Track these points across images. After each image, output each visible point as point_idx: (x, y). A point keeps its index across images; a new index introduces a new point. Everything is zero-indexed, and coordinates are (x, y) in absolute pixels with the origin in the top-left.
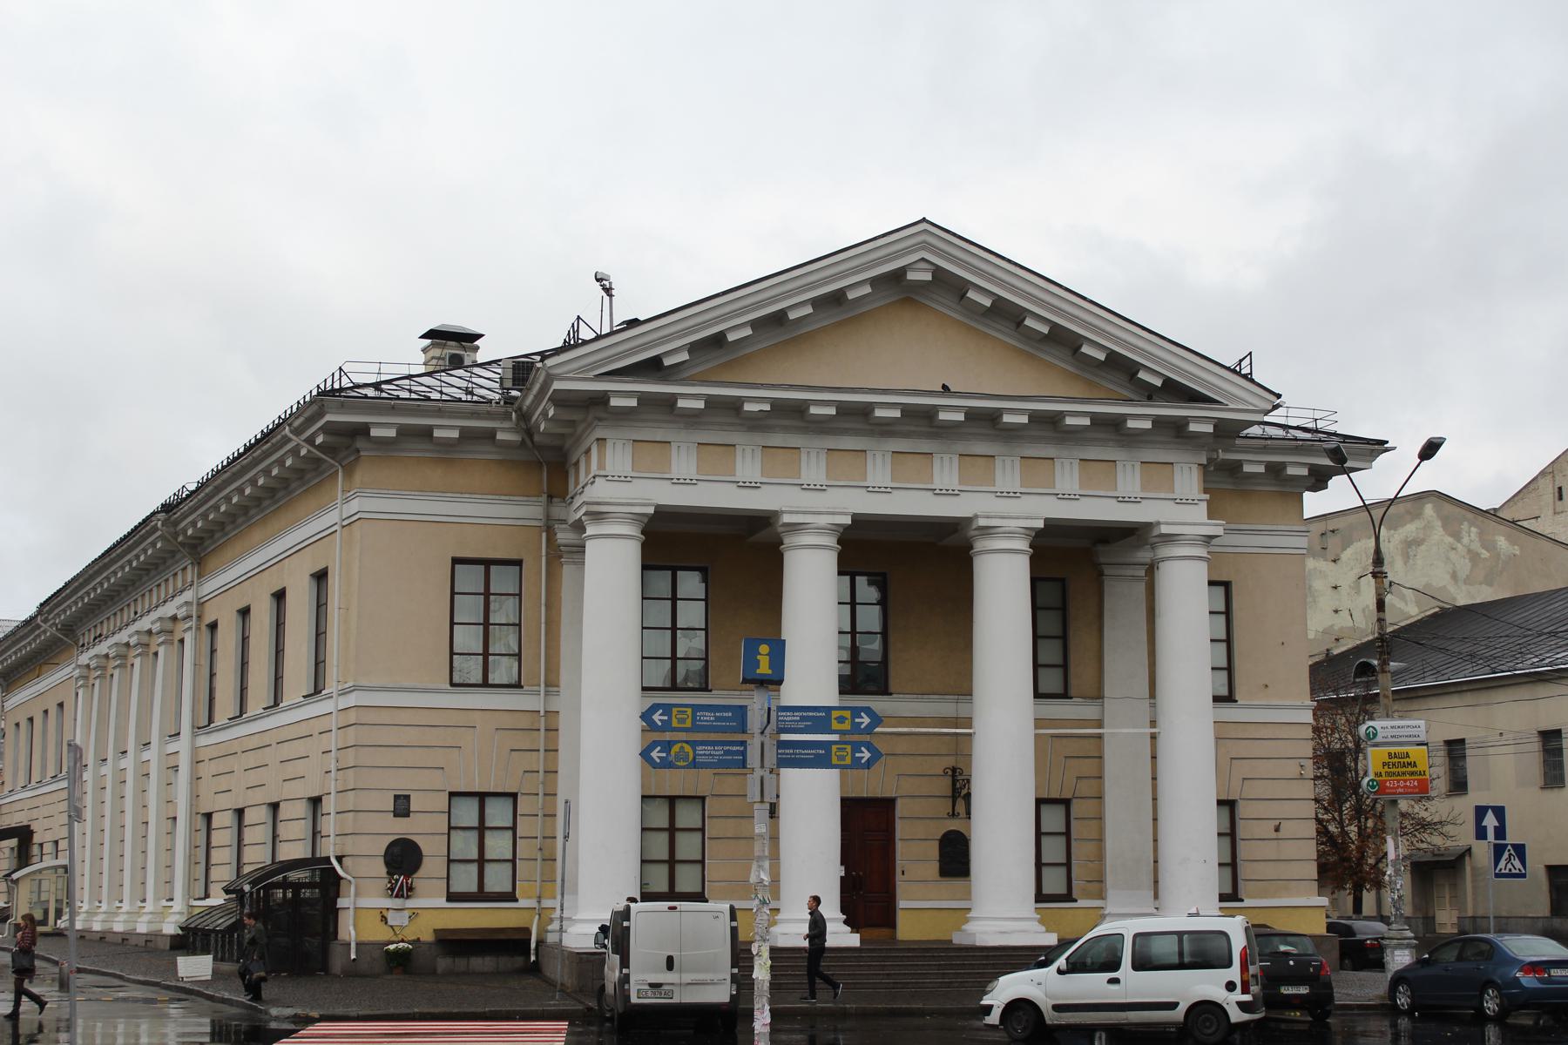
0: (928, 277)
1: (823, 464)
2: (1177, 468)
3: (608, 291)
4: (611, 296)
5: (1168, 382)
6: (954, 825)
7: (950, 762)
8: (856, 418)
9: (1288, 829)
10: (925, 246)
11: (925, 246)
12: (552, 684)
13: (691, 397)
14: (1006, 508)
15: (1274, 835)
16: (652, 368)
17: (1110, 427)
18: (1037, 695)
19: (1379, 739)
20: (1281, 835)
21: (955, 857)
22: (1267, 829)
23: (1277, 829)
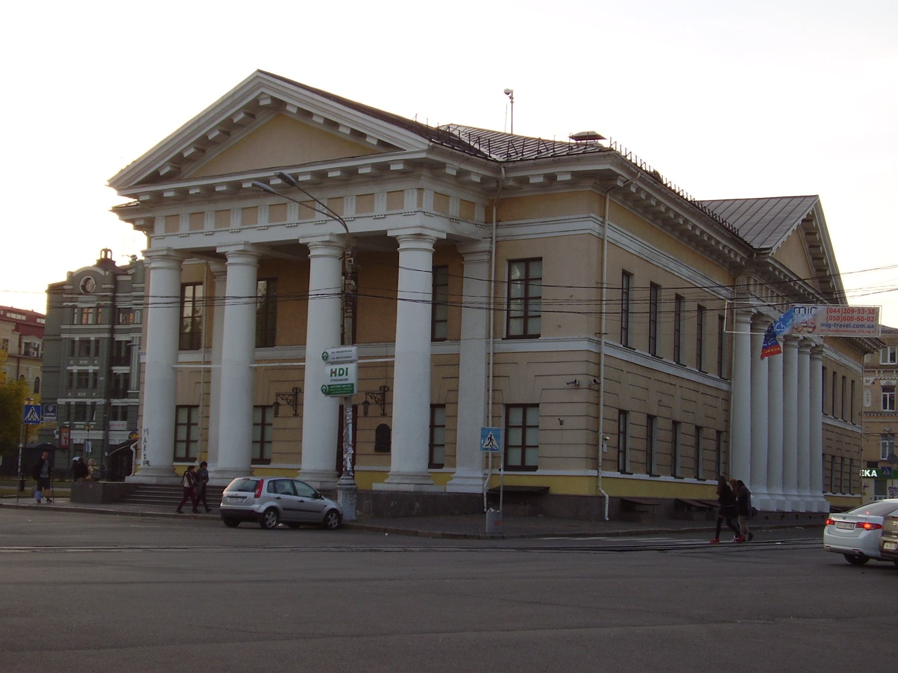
0: (268, 102)
1: (240, 217)
2: (406, 193)
3: (511, 98)
4: (512, 102)
5: (381, 143)
6: (383, 421)
7: (382, 383)
8: (261, 190)
9: (569, 423)
10: (260, 85)
11: (260, 85)
12: (209, 347)
13: (169, 189)
14: (316, 232)
15: (560, 427)
16: (155, 178)
17: (351, 174)
18: (434, 339)
19: (330, 360)
20: (564, 427)
21: (383, 441)
22: (555, 423)
23: (561, 423)
